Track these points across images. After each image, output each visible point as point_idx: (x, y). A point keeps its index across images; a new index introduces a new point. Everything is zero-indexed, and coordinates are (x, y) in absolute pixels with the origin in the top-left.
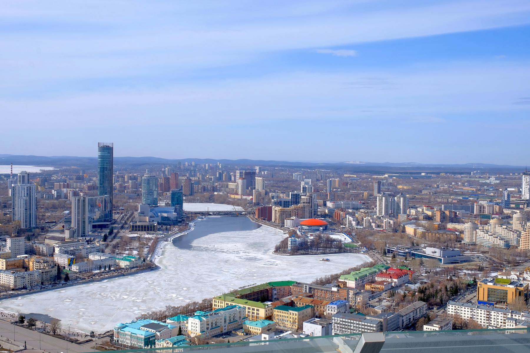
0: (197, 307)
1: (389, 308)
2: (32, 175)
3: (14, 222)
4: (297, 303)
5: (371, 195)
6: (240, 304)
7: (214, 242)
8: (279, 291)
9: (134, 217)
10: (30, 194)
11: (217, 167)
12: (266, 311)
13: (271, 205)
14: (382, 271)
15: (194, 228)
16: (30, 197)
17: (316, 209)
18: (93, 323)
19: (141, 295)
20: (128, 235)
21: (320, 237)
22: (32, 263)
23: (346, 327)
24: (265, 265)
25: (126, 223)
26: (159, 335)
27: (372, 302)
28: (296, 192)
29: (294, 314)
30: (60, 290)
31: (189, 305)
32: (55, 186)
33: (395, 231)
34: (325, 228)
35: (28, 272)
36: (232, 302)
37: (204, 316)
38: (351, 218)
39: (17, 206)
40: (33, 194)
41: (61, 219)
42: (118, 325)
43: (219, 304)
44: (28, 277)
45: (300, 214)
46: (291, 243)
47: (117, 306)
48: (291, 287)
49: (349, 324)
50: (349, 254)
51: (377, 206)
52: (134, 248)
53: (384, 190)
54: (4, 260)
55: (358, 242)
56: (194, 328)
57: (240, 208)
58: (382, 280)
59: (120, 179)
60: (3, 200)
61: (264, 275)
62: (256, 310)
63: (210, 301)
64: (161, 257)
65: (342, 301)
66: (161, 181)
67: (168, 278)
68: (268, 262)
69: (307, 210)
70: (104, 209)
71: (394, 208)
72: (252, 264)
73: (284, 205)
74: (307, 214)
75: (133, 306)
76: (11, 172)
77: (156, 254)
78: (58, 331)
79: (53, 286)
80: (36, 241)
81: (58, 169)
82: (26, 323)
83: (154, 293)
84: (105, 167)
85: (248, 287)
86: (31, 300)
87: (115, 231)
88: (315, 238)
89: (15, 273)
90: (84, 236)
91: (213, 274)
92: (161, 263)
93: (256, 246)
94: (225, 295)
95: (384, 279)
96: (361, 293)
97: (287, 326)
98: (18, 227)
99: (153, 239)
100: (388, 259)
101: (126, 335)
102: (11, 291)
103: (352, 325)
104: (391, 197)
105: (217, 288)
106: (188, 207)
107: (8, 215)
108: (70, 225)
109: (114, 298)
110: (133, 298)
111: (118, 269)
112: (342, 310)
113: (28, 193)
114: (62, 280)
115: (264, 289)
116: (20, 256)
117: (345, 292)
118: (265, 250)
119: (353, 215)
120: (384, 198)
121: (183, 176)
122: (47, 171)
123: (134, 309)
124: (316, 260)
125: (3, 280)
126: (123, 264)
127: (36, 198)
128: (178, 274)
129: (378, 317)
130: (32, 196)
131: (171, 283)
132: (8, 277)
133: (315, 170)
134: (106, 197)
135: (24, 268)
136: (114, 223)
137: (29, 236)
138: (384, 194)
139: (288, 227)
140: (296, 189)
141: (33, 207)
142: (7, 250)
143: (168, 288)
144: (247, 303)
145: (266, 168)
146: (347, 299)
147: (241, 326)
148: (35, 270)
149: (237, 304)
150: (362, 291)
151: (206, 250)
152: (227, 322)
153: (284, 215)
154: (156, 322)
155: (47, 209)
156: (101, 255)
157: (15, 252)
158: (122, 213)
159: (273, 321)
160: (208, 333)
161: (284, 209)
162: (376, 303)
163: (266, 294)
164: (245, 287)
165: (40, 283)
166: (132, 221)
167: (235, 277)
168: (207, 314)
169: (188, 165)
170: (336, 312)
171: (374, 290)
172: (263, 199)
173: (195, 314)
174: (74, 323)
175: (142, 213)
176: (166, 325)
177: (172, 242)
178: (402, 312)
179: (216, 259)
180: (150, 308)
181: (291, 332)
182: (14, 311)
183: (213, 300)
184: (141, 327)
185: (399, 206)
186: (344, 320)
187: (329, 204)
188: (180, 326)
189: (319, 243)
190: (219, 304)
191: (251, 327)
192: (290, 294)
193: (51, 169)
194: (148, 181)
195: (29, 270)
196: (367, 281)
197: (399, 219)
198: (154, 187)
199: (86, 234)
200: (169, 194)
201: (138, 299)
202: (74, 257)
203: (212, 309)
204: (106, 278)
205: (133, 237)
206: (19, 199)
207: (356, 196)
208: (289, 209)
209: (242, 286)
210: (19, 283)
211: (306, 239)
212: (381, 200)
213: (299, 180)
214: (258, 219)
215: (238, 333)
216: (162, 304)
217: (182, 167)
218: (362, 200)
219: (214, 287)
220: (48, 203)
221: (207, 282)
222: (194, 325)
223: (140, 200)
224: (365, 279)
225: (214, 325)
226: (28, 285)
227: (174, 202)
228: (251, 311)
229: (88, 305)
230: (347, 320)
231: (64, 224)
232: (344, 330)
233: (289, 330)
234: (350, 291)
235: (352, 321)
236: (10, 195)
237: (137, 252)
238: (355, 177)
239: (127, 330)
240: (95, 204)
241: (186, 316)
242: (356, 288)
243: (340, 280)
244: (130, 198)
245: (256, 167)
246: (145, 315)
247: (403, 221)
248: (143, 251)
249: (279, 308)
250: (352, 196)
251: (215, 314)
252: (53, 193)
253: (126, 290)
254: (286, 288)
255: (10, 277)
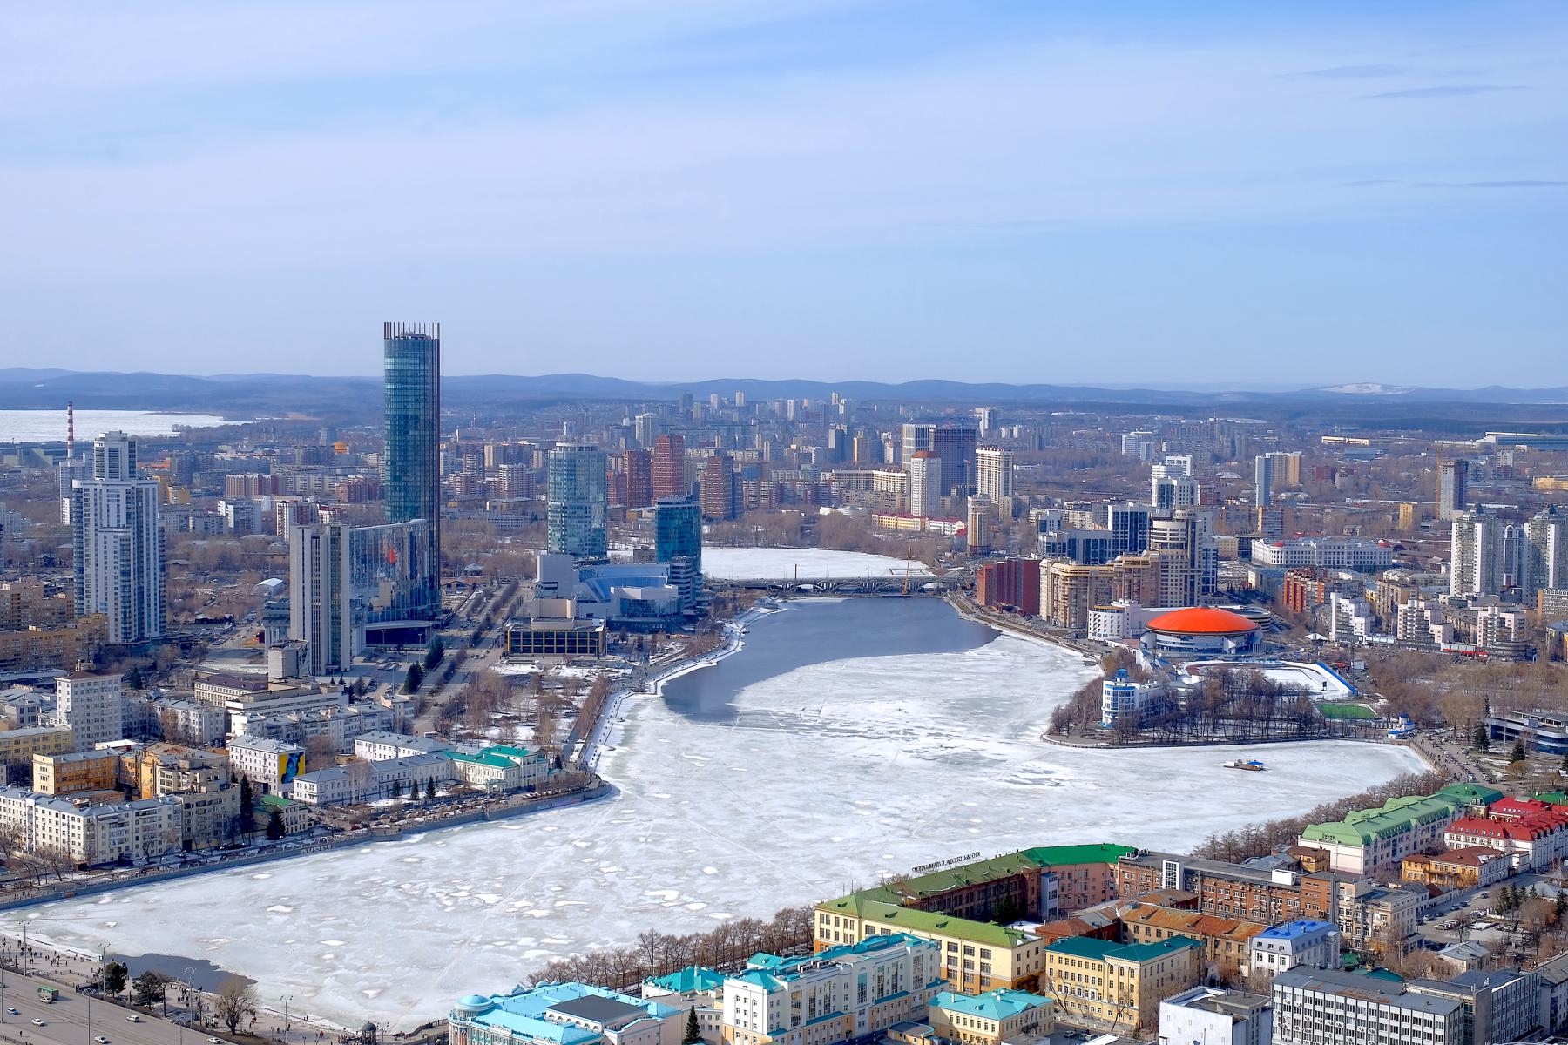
0: (756, 937)
1: (1500, 954)
2: (146, 446)
3: (82, 621)
4: (1137, 929)
5: (1429, 516)
6: (920, 929)
7: (817, 694)
8: (1067, 881)
9: (520, 601)
10: (139, 517)
11: (829, 410)
12: (1019, 956)
13: (1036, 553)
14: (1468, 810)
15: (741, 643)
16: (139, 525)
17: (1211, 569)
18: (371, 993)
19: (548, 893)
20: (497, 669)
21: (1225, 679)
22: (151, 770)
23: (1328, 1022)
24: (1011, 782)
25: (489, 624)
26: (615, 1041)
27: (1430, 931)
28: (1131, 504)
29: (1126, 971)
30: (246, 872)
31: (725, 931)
32: (229, 487)
33: (1525, 653)
34: (1244, 644)
35: (137, 804)
36: (886, 923)
37: (783, 972)
38: (1348, 606)
39: (92, 562)
40: (148, 515)
41: (252, 607)
42: (466, 1001)
43: (840, 929)
44: (137, 822)
45: (1147, 589)
46: (1115, 700)
47: (457, 931)
48: (1112, 866)
49: (1340, 1012)
50: (1341, 742)
51: (1453, 558)
52: (519, 718)
53: (1481, 494)
54: (50, 760)
55: (1376, 699)
56: (746, 1019)
57: (918, 565)
58: (1471, 845)
59: (467, 460)
60: (40, 539)
61: (1011, 823)
62: (977, 953)
63: (805, 916)
64: (619, 749)
65: (1313, 924)
66: (620, 465)
67: (646, 829)
68: (1025, 771)
69: (1175, 574)
70: (407, 573)
71: (1520, 566)
72: (964, 780)
73: (1088, 555)
74: (1175, 590)
75: (515, 935)
76: (68, 434)
77: (603, 738)
78: (245, 1024)
79: (226, 855)
80: (162, 690)
81: (240, 423)
82: (129, 989)
83: (597, 885)
84: (411, 413)
85: (947, 867)
86: (149, 907)
87: (449, 653)
88: (1205, 682)
89: (87, 805)
90: (338, 671)
91: (817, 816)
92: (620, 771)
93: (977, 710)
94: (861, 895)
95: (1478, 839)
96: (1387, 893)
97: (1096, 1015)
98: (97, 636)
99: (589, 684)
100: (1496, 762)
101: (493, 1038)
102: (74, 871)
103: (1349, 1014)
104: (1508, 522)
105: (832, 870)
106: (719, 563)
107: (61, 596)
108: (284, 631)
109: (449, 903)
110: (519, 904)
111: (464, 793)
112: (1314, 957)
113: (131, 511)
114: (259, 833)
115: (1009, 875)
116: (105, 745)
117: (1324, 888)
118: (1014, 728)
119: (1355, 592)
120: (1479, 527)
121: (702, 446)
122: (197, 430)
123: (520, 943)
124: (1211, 765)
125: (47, 832)
126: (481, 776)
127: (162, 530)
128: (682, 814)
129: (1455, 986)
130: (148, 524)
131: (659, 849)
132: (66, 821)
133: (1206, 419)
134: (415, 526)
135: (119, 787)
136: (447, 624)
137: (136, 670)
138: (1480, 510)
139: (1101, 639)
140: (1130, 494)
141: (148, 564)
142: (60, 721)
143: (648, 867)
144: (944, 925)
145: (1018, 412)
146: (1331, 916)
147: (920, 1014)
148: (162, 795)
149: (907, 931)
150: (1391, 886)
151: (789, 726)
152: (871, 995)
153: (1088, 594)
154: (603, 993)
155: (201, 572)
156: (399, 743)
157: (88, 729)
158: (474, 587)
159: (1042, 994)
160: (796, 1035)
161: (1087, 572)
162: (1448, 935)
163: (1017, 892)
164: (937, 864)
165: (180, 843)
166: (511, 616)
167: (899, 827)
168: (793, 964)
169: (721, 406)
170: (1288, 965)
171: (1440, 882)
172: (1007, 532)
173: (751, 966)
174: (303, 992)
175: (550, 586)
176: (639, 1004)
177: (660, 693)
178: (1553, 971)
179: (826, 759)
180: (580, 942)
181: (1115, 1039)
182: (84, 945)
183: (817, 913)
184: (549, 1012)
185: (1539, 559)
186: (1319, 996)
187: (1263, 552)
188: (693, 1012)
189: (1220, 703)
190: (837, 929)
191: (962, 1016)
192: (1111, 893)
193: (214, 421)
194: (571, 467)
195: (139, 795)
196: (1411, 847)
197: (1539, 610)
198: (593, 489)
199: (345, 664)
200: (648, 514)
201: (537, 906)
202: (302, 749)
203: (812, 949)
204: (419, 830)
205: (515, 677)
206: (101, 536)
207: (1369, 520)
208: (1106, 572)
209: (926, 863)
210: (104, 844)
211: (1171, 684)
212: (1467, 535)
213: (1143, 457)
214: (986, 609)
215: (911, 1039)
216: (624, 925)
217: (697, 412)
218: (1393, 533)
219: (819, 864)
220: (205, 551)
221: (792, 847)
222: (747, 1007)
223: (540, 536)
224: (1401, 839)
225: (820, 1008)
226: (135, 851)
227: (666, 546)
228: (959, 955)
229: (354, 925)
230: (1330, 998)
231: (263, 628)
232: (1318, 1033)
233: (1105, 1029)
234: (1342, 885)
235: (1351, 1002)
236: (67, 521)
237: (533, 733)
238: (1365, 446)
239: (497, 1022)
240: (376, 554)
241: (716, 971)
242: (1366, 873)
243: (1303, 843)
244: (503, 530)
245: (977, 409)
246: (563, 966)
247: (1555, 618)
248: (553, 729)
249: (1066, 947)
250: (1354, 518)
251: (824, 965)
252: (223, 513)
253: (492, 874)
254: (1095, 870)
255: (71, 823)
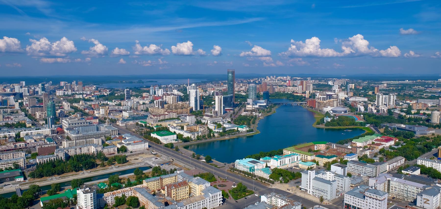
69: (335, 102)
74: (335, 105)
108: (215, 109)
152: (291, 161)
154: (255, 160)
